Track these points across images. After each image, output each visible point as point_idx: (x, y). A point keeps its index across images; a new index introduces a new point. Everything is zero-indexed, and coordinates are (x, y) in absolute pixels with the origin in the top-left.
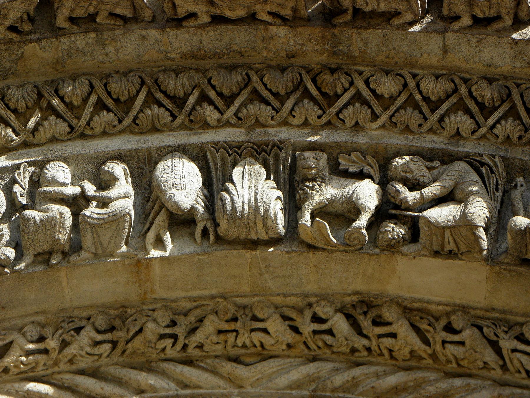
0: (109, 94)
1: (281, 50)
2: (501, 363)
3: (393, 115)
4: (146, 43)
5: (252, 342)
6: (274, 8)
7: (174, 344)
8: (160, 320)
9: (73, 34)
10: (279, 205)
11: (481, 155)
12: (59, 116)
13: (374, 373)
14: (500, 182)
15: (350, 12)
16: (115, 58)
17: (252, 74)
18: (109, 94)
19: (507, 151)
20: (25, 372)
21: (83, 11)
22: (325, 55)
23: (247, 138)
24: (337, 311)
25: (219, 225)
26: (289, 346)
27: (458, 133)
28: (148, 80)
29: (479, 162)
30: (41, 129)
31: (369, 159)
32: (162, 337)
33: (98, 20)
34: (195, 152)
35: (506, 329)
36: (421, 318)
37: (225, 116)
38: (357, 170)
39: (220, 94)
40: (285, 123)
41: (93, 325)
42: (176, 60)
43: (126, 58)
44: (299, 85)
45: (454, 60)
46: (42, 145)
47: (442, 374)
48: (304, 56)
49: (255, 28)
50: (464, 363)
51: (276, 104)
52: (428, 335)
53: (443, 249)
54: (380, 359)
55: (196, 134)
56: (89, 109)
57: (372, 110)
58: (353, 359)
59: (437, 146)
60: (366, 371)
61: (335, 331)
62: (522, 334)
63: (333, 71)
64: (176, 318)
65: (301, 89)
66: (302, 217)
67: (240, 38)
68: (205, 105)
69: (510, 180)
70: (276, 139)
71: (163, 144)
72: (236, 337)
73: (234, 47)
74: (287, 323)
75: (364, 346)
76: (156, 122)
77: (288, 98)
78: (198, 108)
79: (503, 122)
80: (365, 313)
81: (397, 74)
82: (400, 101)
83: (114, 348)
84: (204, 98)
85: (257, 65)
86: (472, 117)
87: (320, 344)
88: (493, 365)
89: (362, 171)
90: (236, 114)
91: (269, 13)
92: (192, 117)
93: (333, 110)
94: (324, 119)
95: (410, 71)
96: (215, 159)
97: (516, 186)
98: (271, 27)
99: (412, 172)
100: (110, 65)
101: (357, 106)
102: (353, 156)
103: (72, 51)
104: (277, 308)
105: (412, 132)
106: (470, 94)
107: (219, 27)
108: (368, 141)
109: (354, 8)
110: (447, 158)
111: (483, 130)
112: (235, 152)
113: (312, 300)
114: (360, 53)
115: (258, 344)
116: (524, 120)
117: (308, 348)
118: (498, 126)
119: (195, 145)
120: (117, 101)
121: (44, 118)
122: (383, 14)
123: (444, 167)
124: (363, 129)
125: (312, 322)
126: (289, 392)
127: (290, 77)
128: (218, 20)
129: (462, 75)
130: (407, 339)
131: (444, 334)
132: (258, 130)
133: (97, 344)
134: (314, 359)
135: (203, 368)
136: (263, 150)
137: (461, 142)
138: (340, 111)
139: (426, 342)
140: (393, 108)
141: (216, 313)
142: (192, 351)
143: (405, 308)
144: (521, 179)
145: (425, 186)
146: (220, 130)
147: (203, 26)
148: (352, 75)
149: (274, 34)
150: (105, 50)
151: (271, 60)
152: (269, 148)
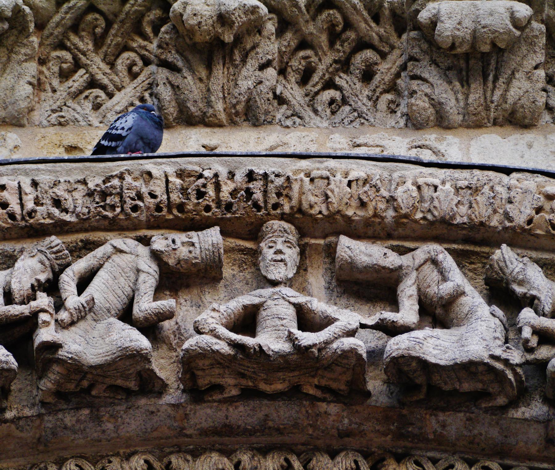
4: (156, 418)
6: (324, 382)
9: (60, 410)
15: (424, 390)
16: (113, 435)
21: (73, 386)
22: (389, 436)
42: (194, 436)
43: (128, 435)
48: (362, 437)
49: (299, 404)
73: (270, 424)
95: (500, 461)
98: (319, 404)
100: (107, 442)
103: (58, 429)
114: (435, 436)
128: (249, 394)
148: (425, 466)
150: (101, 426)
151: (318, 439)
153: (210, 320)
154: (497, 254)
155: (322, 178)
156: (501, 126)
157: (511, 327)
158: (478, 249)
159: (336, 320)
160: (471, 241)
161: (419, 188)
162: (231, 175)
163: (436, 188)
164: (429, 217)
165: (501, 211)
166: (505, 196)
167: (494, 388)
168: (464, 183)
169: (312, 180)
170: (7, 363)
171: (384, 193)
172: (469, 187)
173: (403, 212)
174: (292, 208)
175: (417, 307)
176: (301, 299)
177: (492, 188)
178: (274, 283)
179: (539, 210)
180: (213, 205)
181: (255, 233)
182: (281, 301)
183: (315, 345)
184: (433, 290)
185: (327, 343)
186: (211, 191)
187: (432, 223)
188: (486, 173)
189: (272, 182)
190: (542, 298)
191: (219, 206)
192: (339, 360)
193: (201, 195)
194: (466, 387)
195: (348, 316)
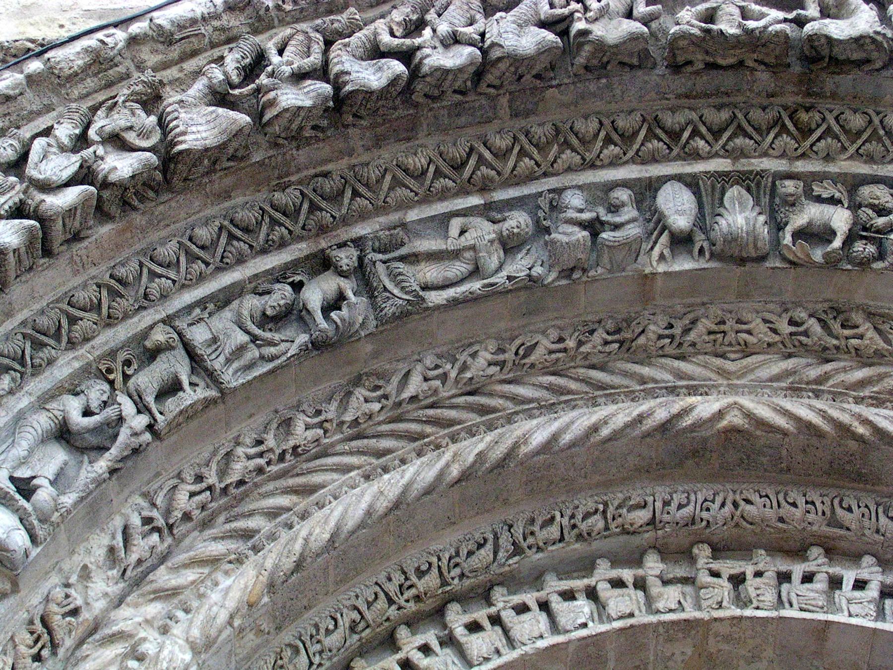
0: (616, 130)
3: (859, 148)
7: (671, 343)
8: (660, 323)
12: (574, 150)
15: (827, 60)
17: (737, 111)
18: (616, 130)
20: (548, 367)
23: (735, 169)
24: (811, 316)
26: (769, 345)
28: (648, 118)
30: (558, 160)
31: (839, 185)
32: (660, 337)
33: (609, 68)
34: (689, 180)
36: (883, 322)
37: (714, 150)
40: (765, 154)
41: (604, 327)
44: (778, 121)
46: (559, 174)
51: (757, 137)
54: (846, 357)
55: (689, 164)
56: (599, 144)
60: (836, 367)
63: (807, 110)
64: (673, 321)
67: (728, 80)
68: (697, 139)
70: (758, 169)
71: (662, 174)
72: (724, 337)
73: (722, 89)
74: (767, 325)
76: (656, 154)
77: (768, 133)
78: (691, 142)
80: (835, 318)
81: (864, 113)
82: (865, 136)
83: (620, 348)
84: (695, 133)
87: (797, 343)
89: (833, 196)
90: (723, 147)
91: (756, 61)
92: (687, 150)
93: (808, 143)
94: (800, 151)
101: (829, 140)
104: (758, 312)
105: (875, 163)
107: (711, 72)
109: (830, 58)
113: (789, 306)
115: (742, 343)
119: (689, 175)
120: (622, 136)
121: (561, 152)
122: (853, 62)
127: (771, 115)
128: (712, 66)
130: (872, 339)
132: (743, 160)
133: (606, 343)
134: (790, 356)
135: (695, 363)
138: (812, 146)
140: (860, 142)
142: (686, 348)
143: (870, 313)
147: (697, 73)
159: (768, 15)
167: (875, 55)
170: (556, 43)
175: (819, 9)
194: (856, 56)
195: (775, 14)
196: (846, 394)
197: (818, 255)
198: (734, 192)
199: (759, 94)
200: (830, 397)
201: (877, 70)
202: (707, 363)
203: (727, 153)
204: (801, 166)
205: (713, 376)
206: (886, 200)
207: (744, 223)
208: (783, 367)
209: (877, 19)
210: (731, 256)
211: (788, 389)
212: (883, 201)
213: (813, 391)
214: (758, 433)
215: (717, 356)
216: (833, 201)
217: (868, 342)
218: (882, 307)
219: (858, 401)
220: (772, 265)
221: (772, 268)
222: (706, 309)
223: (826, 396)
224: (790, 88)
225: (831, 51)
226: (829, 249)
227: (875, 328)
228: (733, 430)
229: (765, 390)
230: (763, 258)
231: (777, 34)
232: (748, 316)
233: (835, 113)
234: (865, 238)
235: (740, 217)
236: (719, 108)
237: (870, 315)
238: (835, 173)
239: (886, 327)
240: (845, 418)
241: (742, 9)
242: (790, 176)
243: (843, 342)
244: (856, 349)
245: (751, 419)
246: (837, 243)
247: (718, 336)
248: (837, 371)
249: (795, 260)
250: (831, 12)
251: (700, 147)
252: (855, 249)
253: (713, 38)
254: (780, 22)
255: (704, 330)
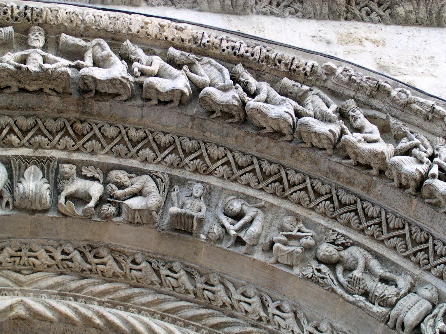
1: (55, 109)
2: (160, 282)
3: (112, 148)
5: (29, 263)
10: (48, 192)
11: (157, 172)
13: (92, 283)
14: (166, 187)
15: (94, 92)
17: (38, 120)
19: (171, 171)
23: (34, 155)
24: (75, 249)
25: (15, 201)
26: (48, 266)
27: (146, 159)
29: (156, 176)
31: (98, 169)
34: (5, 160)
35: (164, 264)
36: (120, 256)
37: (22, 142)
38: (91, 176)
39: (20, 130)
40: (54, 148)
44: (63, 127)
45: (146, 121)
47: (129, 286)
50: (141, 281)
51: (50, 137)
52: (123, 265)
53: (134, 221)
55: (6, 150)
57: (102, 144)
58: (82, 275)
59: (134, 166)
60: (88, 282)
61: (74, 260)
62: (172, 267)
63: (82, 122)
65: (64, 130)
66: (60, 199)
67: (33, 100)
68: (12, 135)
69: (171, 186)
70: (49, 156)
72: (20, 260)
73: (30, 106)
74: (49, 254)
75: (88, 268)
77: (57, 134)
78: (8, 136)
79: (170, 155)
80: (90, 251)
82: (116, 141)
84: (11, 131)
85: (41, 116)
86: (154, 152)
87: (65, 266)
88: (156, 283)
89: (94, 176)
91: (50, 89)
92: (4, 141)
93: (81, 143)
94: (76, 147)
96: (15, 164)
97: (174, 190)
99: (121, 179)
101: (94, 141)
102: (89, 168)
104: (43, 245)
105: (122, 157)
106: (154, 139)
107: (22, 94)
108: (98, 160)
110: (139, 172)
111: (159, 159)
112: (26, 161)
113: (63, 242)
115: (32, 264)
116: (181, 155)
117: (58, 267)
118: (167, 157)
119: (5, 156)
122: (110, 95)
123: (138, 177)
124: (96, 154)
125: (62, 254)
126: (47, 290)
127: (59, 123)
128: (22, 90)
129: (150, 129)
130: (111, 266)
131: (131, 265)
134: (61, 274)
136: (42, 161)
137: (148, 165)
139: (121, 268)
140: (113, 144)
141: (10, 246)
143: (112, 250)
144: (177, 186)
145: (127, 187)
146: (19, 149)
147: (14, 94)
149: (52, 100)
152: (45, 161)
153: (7, 58)
154: (125, 43)
155: (55, 10)
156: (127, 5)
157: (130, 71)
158: (117, 43)
159: (59, 61)
160: (115, 39)
161: (94, 17)
162: (18, 8)
163: (101, 17)
164: (98, 28)
165: (127, 27)
166: (129, 22)
167: (122, 91)
168: (112, 16)
169: (51, 11)
171: (80, 17)
172: (114, 18)
173: (88, 25)
174: (43, 21)
175: (92, 61)
176: (44, 53)
177: (124, 19)
178: (34, 48)
179: (142, 28)
180: (10, 18)
181: (27, 31)
182: (37, 54)
183: (50, 68)
184: (99, 55)
185: (55, 68)
186: (9, 12)
187: (99, 30)
188: (121, 13)
189: (35, 10)
190: (142, 60)
191: (12, 18)
192: (60, 76)
193: (5, 13)
194: (111, 91)
196: (93, 299)
197: (79, 211)
198: (32, 168)
199: (53, 110)
200: (83, 300)
201: (125, 101)
202: (8, 276)
203: (30, 145)
204: (76, 156)
205: (10, 284)
206: (125, 180)
207: (34, 187)
208: (56, 280)
209: (125, 69)
210: (26, 208)
211: (59, 294)
212: (123, 180)
213: (73, 296)
214: (35, 321)
215: (16, 271)
216: (93, 179)
217: (109, 267)
218: (120, 246)
219: (101, 304)
220: (51, 216)
221: (51, 217)
222: (10, 241)
223: (80, 300)
224: (72, 108)
225: (96, 87)
226: (86, 207)
227: (115, 259)
228: (19, 318)
229: (43, 295)
230: (46, 211)
231: (62, 73)
232: (34, 248)
233: (99, 125)
234: (109, 202)
235: (33, 184)
236: (27, 117)
237: (112, 251)
238: (96, 162)
239: (120, 259)
240: (89, 313)
241: (44, 57)
242: (68, 162)
243: (94, 267)
244: (102, 272)
245: (31, 311)
246: (92, 204)
247: (16, 259)
248: (89, 285)
249: (66, 213)
250: (100, 64)
251: (13, 140)
252: (103, 209)
253: (22, 72)
254: (66, 67)
255: (7, 255)
